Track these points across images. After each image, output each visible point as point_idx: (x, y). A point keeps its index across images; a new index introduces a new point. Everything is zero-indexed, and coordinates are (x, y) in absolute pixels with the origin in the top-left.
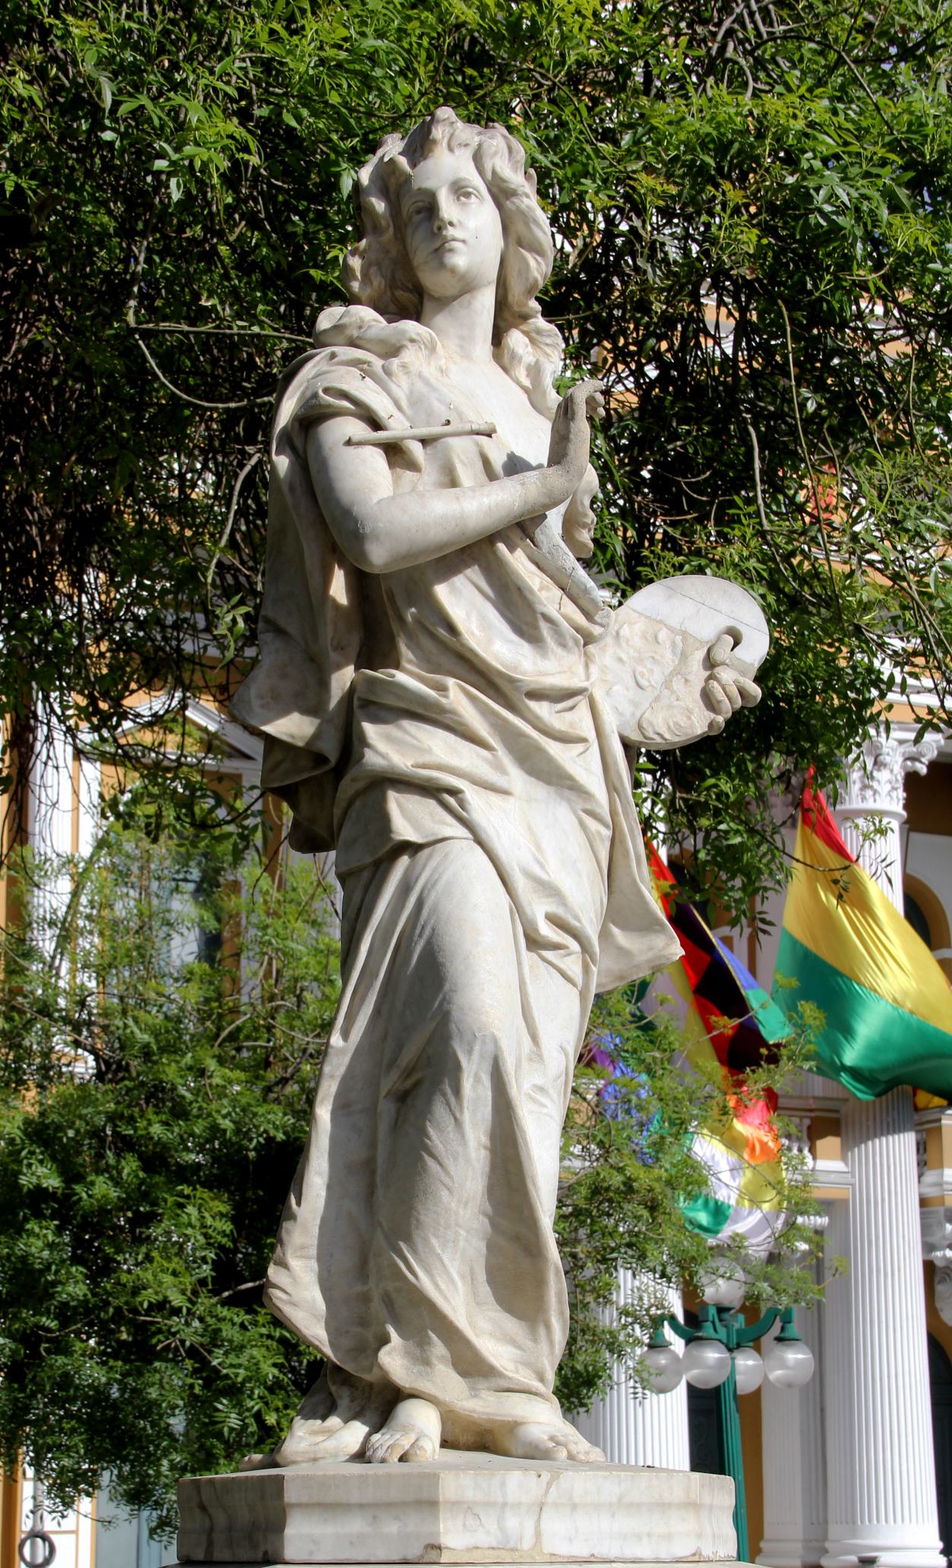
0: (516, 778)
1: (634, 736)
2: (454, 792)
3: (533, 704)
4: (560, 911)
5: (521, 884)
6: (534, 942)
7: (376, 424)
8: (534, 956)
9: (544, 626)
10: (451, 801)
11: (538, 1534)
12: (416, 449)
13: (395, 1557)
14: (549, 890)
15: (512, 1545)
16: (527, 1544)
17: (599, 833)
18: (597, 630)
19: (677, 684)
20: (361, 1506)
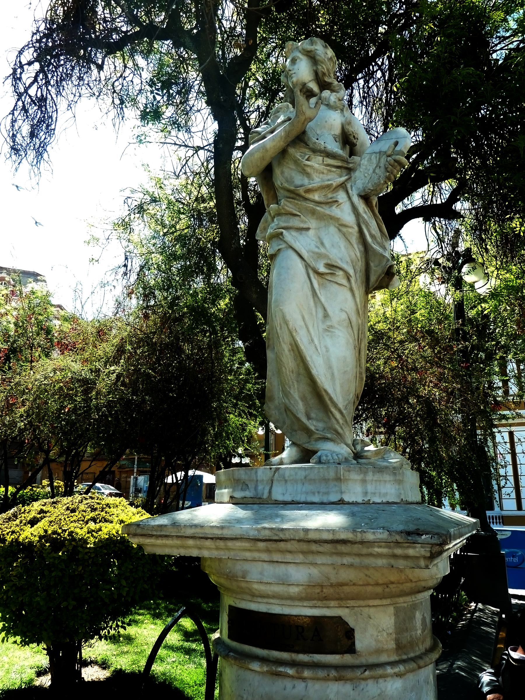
0: (312, 223)
1: (363, 194)
3: (310, 196)
4: (329, 262)
5: (305, 255)
8: (320, 280)
11: (270, 492)
14: (320, 256)
15: (259, 496)
16: (265, 496)
18: (351, 165)
19: (377, 171)
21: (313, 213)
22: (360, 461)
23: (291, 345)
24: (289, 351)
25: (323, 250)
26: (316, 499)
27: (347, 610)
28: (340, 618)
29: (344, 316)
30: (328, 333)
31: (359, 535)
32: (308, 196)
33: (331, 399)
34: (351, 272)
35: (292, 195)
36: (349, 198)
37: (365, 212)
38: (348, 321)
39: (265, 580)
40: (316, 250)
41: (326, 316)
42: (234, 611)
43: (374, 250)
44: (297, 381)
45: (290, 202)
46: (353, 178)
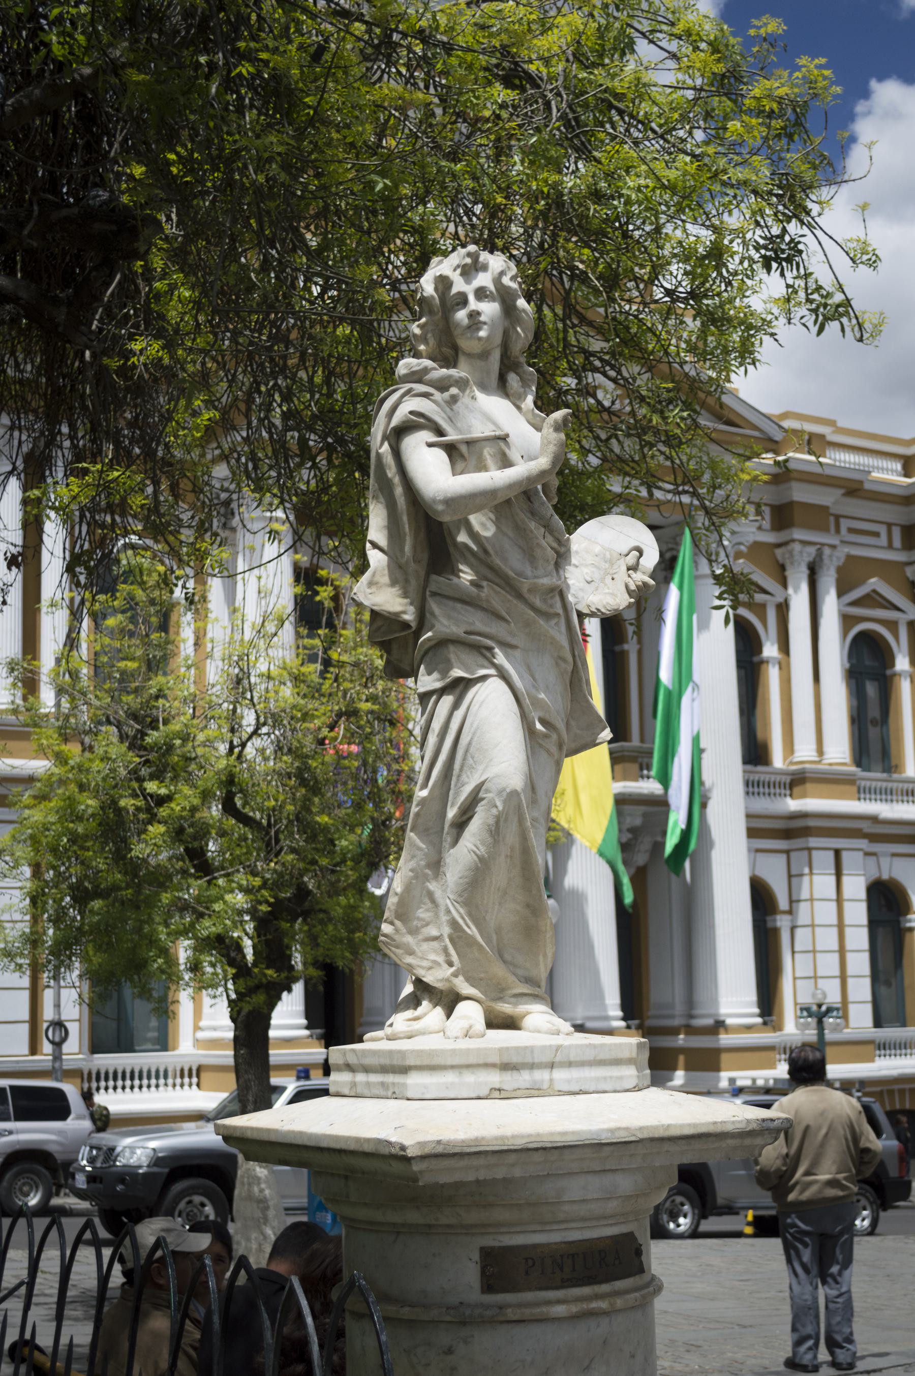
2: (490, 649)
4: (547, 717)
5: (527, 701)
7: (440, 432)
10: (488, 655)
12: (464, 449)
13: (473, 1096)
20: (453, 1067)
21: (527, 624)
23: (512, 849)
24: (507, 856)
35: (497, 580)
39: (589, 1197)
42: (489, 1256)
44: (500, 904)
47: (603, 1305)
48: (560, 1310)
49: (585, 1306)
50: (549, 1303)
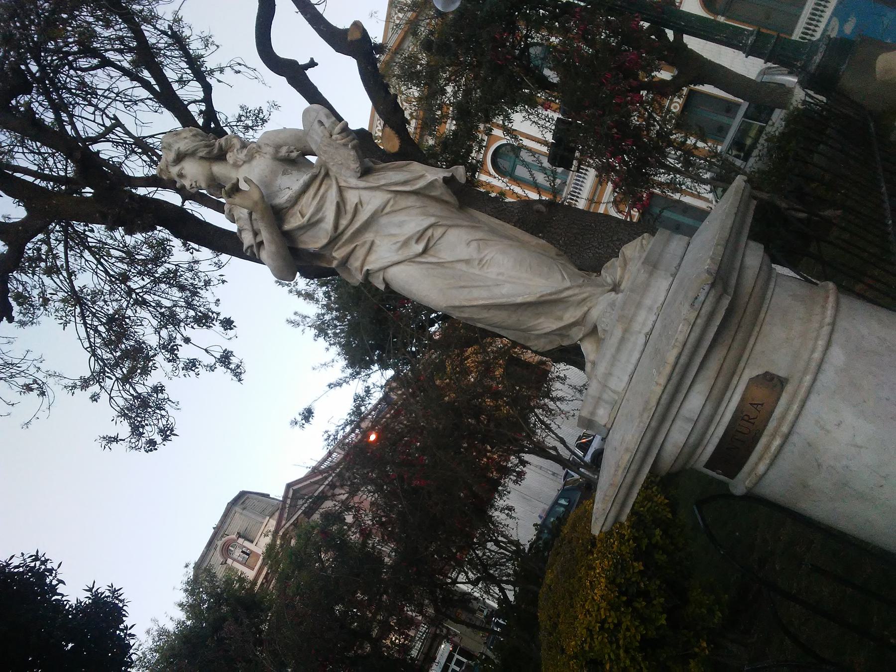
0: (369, 236)
3: (341, 228)
4: (416, 238)
6: (425, 251)
8: (431, 252)
9: (312, 221)
11: (614, 392)
12: (259, 239)
14: (406, 243)
17: (392, 206)
18: (323, 172)
22: (622, 287)
25: (402, 239)
26: (636, 355)
27: (747, 371)
28: (751, 380)
29: (474, 244)
30: (485, 267)
31: (677, 344)
32: (340, 231)
33: (550, 294)
34: (432, 220)
36: (358, 188)
37: (378, 179)
38: (481, 242)
40: (399, 245)
41: (467, 262)
43: (421, 189)
45: (339, 248)
46: (338, 176)
47: (777, 442)
48: (761, 468)
49: (770, 455)
50: (757, 464)
